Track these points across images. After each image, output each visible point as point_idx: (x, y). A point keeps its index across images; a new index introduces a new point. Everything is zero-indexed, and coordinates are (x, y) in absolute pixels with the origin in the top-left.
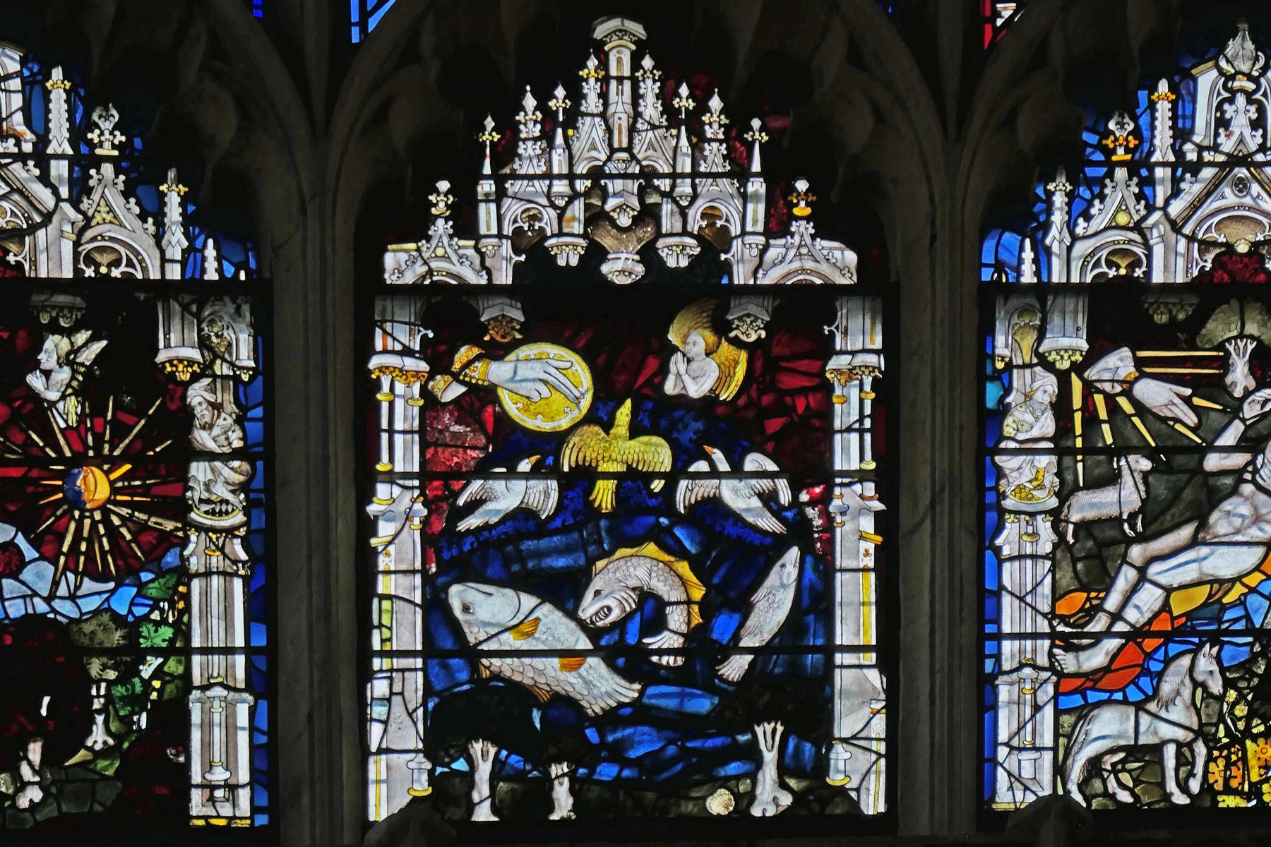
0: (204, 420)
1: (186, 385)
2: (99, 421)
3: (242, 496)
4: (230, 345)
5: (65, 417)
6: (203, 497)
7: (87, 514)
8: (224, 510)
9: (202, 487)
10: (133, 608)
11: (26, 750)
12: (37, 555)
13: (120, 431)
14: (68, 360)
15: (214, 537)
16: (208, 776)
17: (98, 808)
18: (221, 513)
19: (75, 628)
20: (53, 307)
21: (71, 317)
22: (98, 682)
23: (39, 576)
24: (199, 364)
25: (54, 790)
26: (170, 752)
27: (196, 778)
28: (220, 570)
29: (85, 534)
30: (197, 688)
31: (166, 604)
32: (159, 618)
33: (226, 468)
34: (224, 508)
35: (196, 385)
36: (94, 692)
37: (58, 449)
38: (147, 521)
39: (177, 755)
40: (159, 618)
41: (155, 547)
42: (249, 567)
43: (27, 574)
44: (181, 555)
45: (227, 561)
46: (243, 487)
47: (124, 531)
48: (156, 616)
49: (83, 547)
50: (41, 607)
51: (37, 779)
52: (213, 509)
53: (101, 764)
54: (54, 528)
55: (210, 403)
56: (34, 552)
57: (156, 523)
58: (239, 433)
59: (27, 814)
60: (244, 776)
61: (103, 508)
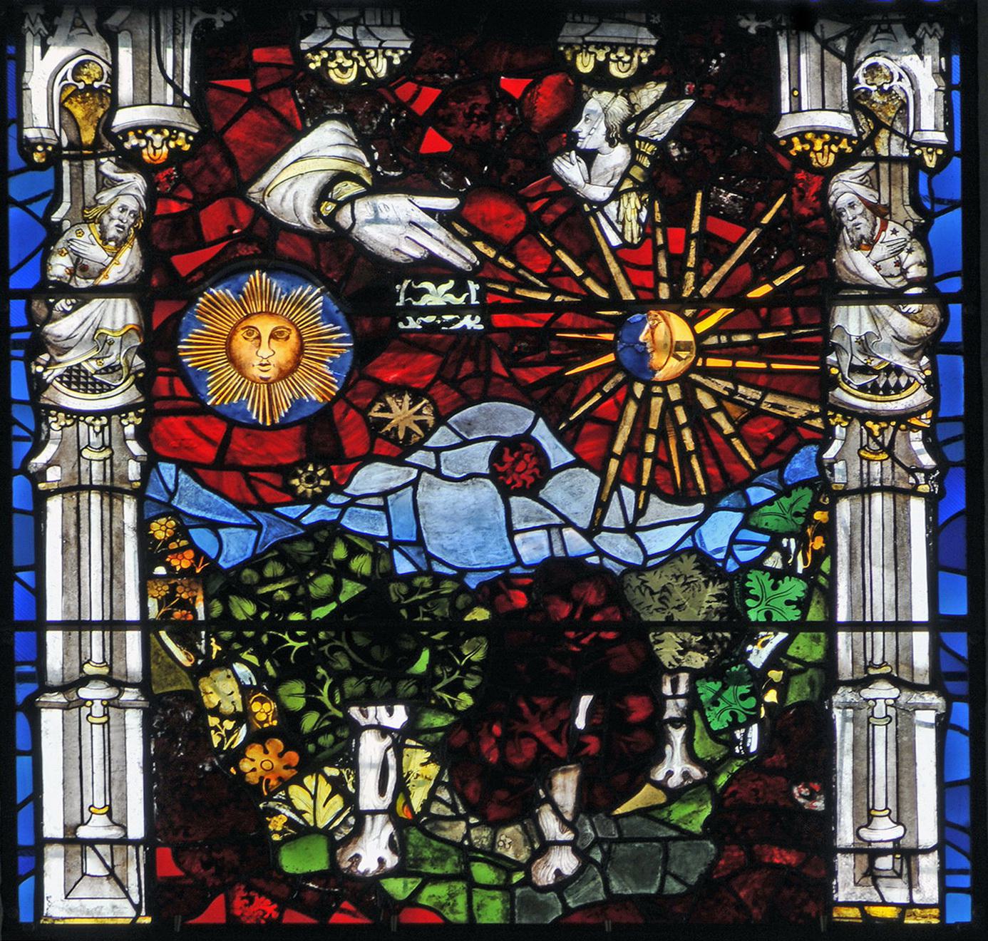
0: (859, 232)
1: (828, 174)
2: (677, 233)
3: (925, 360)
4: (904, 106)
5: (619, 227)
6: (856, 362)
7: (657, 390)
8: (892, 384)
9: (855, 346)
10: (736, 547)
11: (549, 787)
12: (571, 458)
13: (713, 250)
14: (623, 134)
15: (876, 428)
16: (865, 833)
17: (674, 887)
18: (887, 390)
19: (635, 582)
20: (600, 46)
21: (630, 62)
22: (675, 672)
23: (576, 494)
24: (850, 138)
25: (597, 856)
26: (799, 792)
27: (845, 836)
28: (887, 484)
29: (653, 424)
30: (847, 684)
31: (792, 541)
32: (779, 566)
33: (896, 314)
34: (892, 382)
35: (846, 175)
36: (667, 689)
37: (609, 283)
38: (759, 402)
39: (811, 798)
40: (779, 566)
41: (772, 447)
42: (936, 480)
43: (554, 490)
44: (819, 460)
45: (899, 469)
46: (930, 346)
47: (720, 418)
48: (774, 561)
49: (650, 445)
50: (576, 544)
51: (569, 836)
52: (875, 383)
53: (679, 812)
54: (599, 413)
55: (868, 205)
56: (567, 453)
57: (774, 406)
58: (919, 255)
59: (552, 895)
60: (928, 833)
61: (683, 379)
